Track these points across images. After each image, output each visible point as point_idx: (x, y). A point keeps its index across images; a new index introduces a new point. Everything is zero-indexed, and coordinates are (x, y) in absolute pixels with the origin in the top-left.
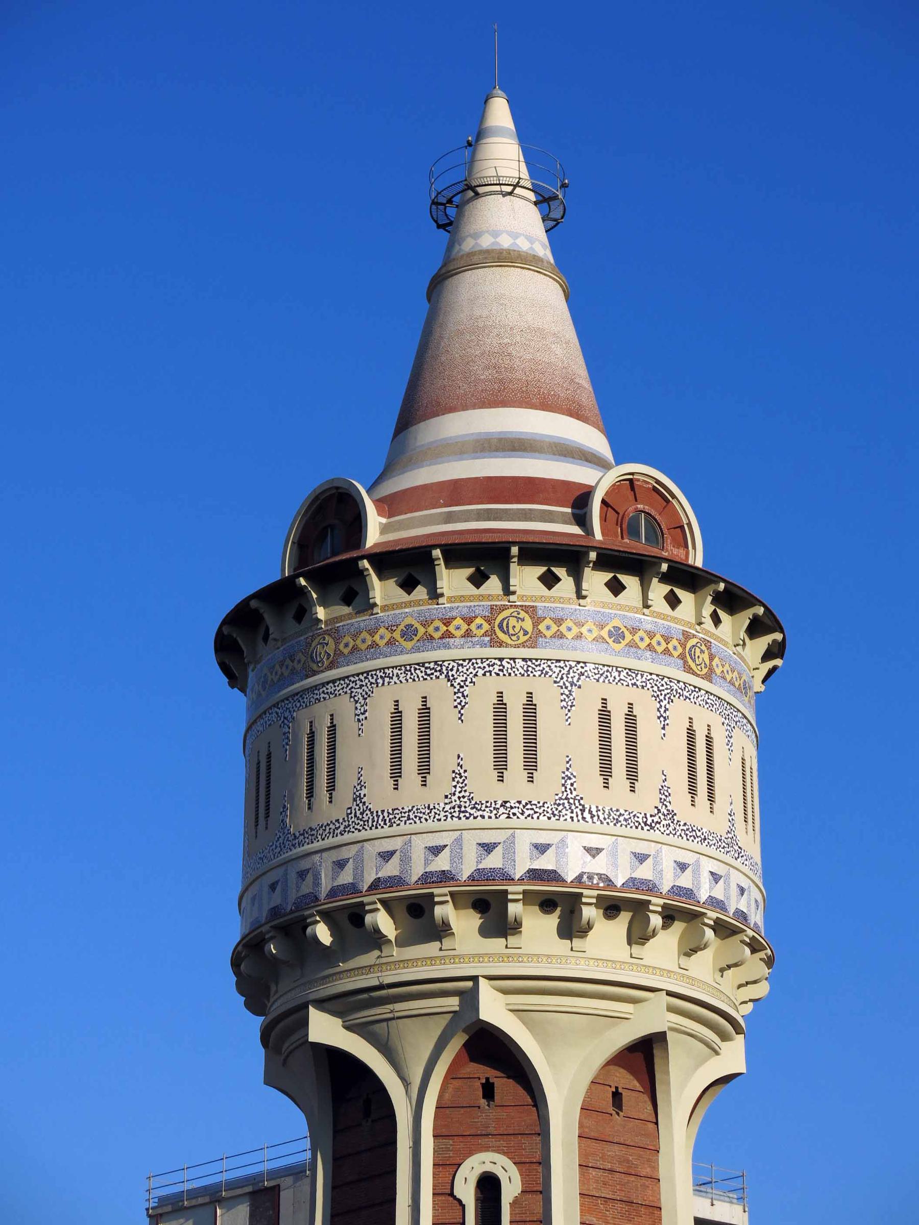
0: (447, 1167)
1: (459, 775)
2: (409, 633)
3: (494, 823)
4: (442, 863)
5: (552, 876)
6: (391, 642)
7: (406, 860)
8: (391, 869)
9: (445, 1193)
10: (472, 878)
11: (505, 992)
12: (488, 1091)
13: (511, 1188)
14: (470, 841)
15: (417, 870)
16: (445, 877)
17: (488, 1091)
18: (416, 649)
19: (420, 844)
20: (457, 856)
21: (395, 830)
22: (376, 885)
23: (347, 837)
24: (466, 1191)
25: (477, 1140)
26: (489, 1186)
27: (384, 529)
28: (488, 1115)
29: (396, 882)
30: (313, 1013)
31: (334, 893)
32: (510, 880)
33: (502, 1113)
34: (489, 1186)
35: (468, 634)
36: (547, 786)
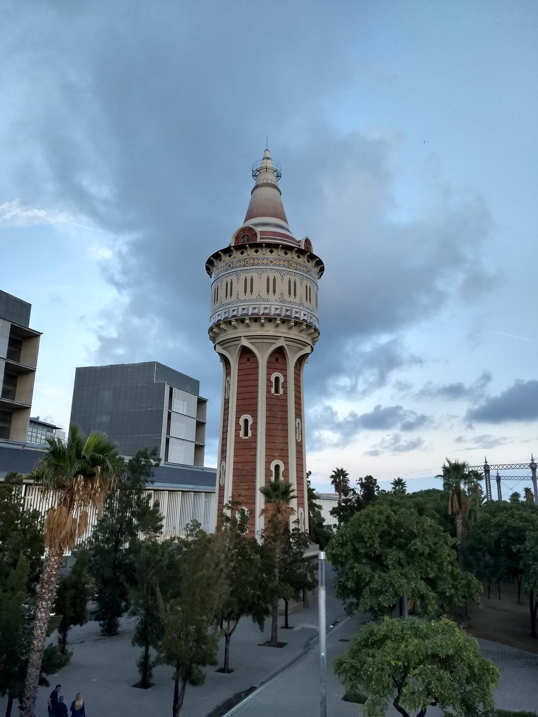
0: (269, 374)
1: (282, 294)
2: (271, 262)
3: (288, 305)
4: (278, 312)
5: (298, 318)
6: (267, 263)
7: (270, 310)
8: (267, 311)
9: (268, 380)
10: (284, 316)
11: (286, 340)
12: (277, 360)
13: (282, 380)
14: (284, 308)
15: (273, 312)
16: (279, 315)
17: (277, 360)
18: (273, 266)
19: (273, 307)
20: (281, 311)
21: (268, 303)
22: (263, 314)
23: (256, 303)
24: (273, 380)
25: (276, 370)
26: (277, 379)
27: (261, 238)
28: (277, 365)
29: (267, 314)
30: (243, 338)
31: (252, 314)
32: (291, 318)
33: (279, 365)
34: (277, 379)
35: (284, 265)
36: (297, 300)
